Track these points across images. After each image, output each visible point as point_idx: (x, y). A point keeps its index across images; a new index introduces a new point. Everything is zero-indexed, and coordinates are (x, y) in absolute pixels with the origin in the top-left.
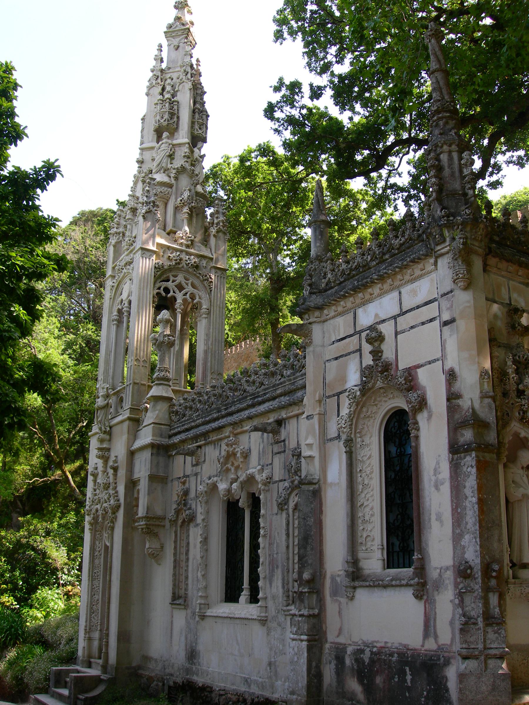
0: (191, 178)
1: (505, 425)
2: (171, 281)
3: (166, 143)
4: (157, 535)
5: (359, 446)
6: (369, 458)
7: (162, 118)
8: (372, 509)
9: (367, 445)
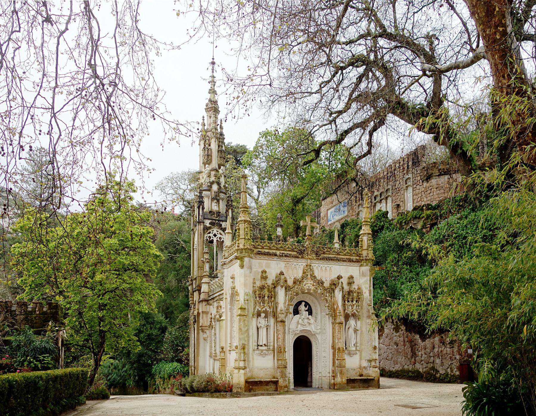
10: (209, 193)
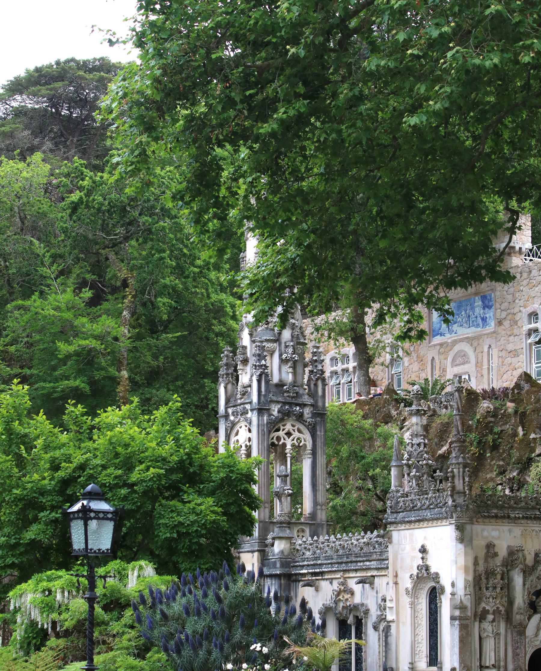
1: (479, 604)
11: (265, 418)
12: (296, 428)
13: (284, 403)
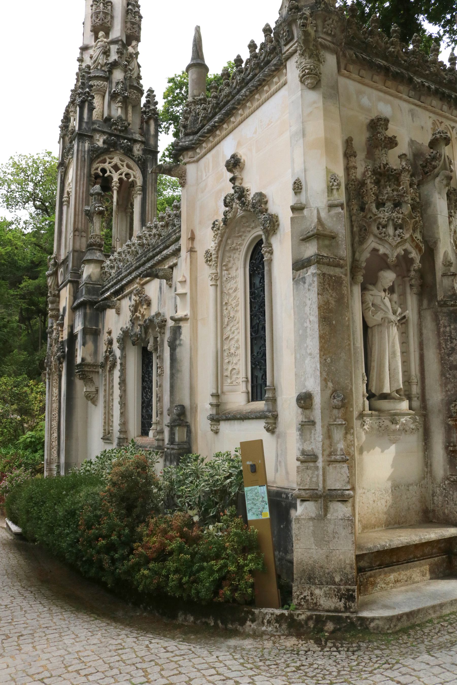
0: (125, 72)
1: (362, 241)
2: (107, 163)
3: (102, 41)
4: (92, 380)
5: (225, 279)
6: (235, 291)
7: (97, 18)
8: (237, 341)
9: (233, 278)
10: (105, 83)
11: (87, 145)
12: (125, 164)
13: (111, 135)
